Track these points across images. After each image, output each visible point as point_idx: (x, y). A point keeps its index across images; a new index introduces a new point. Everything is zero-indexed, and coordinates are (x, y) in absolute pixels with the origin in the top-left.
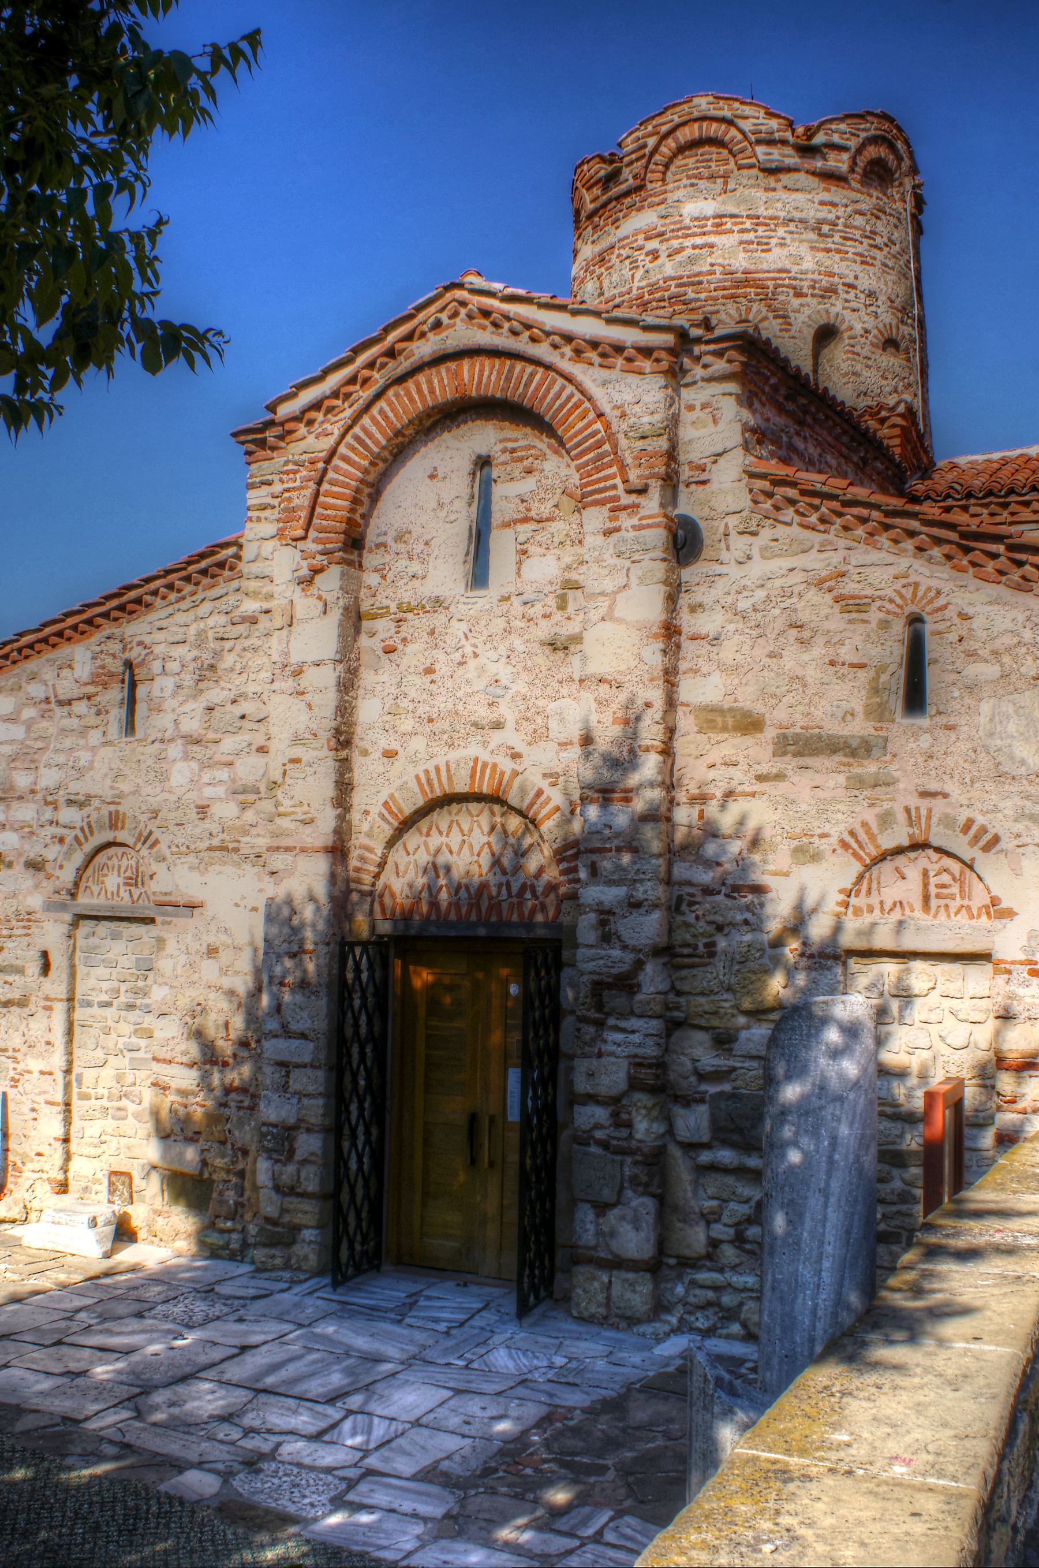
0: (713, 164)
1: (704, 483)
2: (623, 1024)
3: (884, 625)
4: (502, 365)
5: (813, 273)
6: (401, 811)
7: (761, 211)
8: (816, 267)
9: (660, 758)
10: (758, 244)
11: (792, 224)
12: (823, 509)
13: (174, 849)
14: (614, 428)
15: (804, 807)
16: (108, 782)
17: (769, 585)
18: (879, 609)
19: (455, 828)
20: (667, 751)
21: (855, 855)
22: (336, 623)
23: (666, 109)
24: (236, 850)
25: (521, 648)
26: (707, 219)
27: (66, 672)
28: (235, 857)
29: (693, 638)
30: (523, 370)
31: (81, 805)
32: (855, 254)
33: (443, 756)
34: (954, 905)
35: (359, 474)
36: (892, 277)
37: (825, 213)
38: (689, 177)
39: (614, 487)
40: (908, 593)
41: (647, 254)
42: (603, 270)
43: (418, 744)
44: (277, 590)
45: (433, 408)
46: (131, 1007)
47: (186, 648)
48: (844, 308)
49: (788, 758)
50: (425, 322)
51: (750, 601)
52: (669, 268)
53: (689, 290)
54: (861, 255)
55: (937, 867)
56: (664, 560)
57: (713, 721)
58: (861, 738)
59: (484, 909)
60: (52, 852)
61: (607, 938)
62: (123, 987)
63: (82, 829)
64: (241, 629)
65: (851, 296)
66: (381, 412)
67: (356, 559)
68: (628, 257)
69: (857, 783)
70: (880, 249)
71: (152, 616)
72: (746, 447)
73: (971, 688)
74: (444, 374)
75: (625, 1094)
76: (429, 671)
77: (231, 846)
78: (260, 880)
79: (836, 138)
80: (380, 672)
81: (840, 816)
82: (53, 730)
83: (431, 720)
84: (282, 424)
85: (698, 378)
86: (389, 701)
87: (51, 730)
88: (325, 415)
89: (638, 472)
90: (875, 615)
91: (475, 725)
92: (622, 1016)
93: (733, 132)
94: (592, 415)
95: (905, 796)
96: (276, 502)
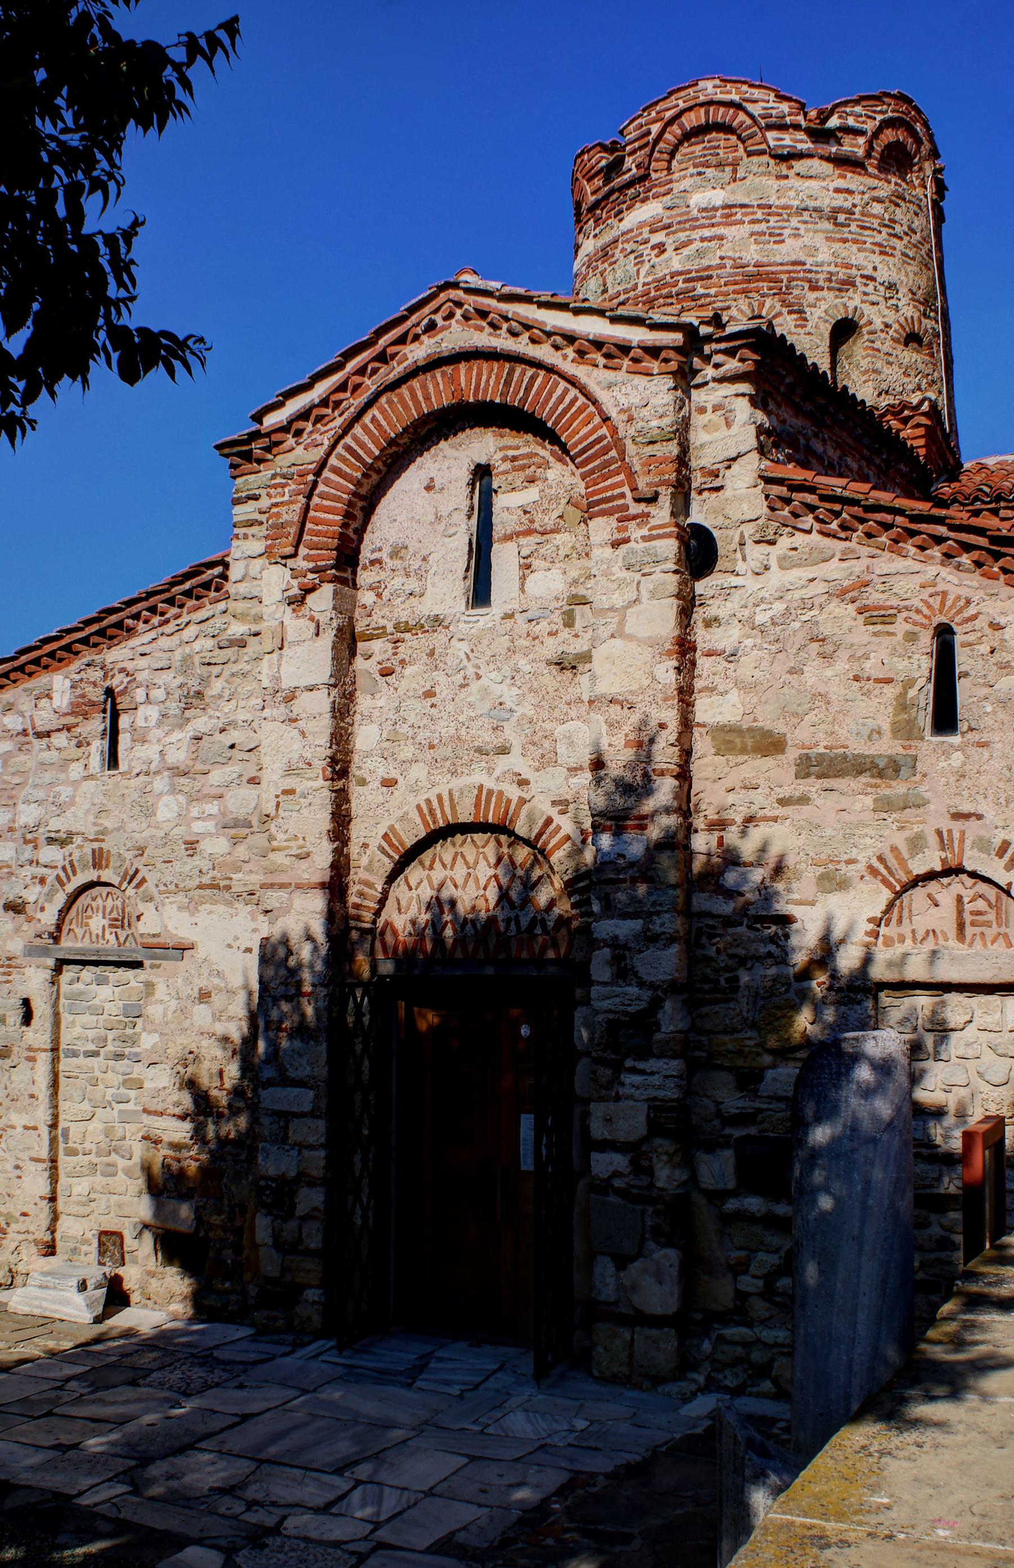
0: (721, 152)
1: (718, 489)
2: (641, 1065)
3: (911, 637)
5: (829, 265)
6: (402, 844)
8: (832, 259)
9: (676, 783)
10: (771, 235)
11: (805, 213)
12: (844, 515)
13: (162, 888)
14: (621, 434)
15: (829, 832)
16: (91, 818)
17: (788, 596)
18: (906, 620)
19: (459, 860)
20: (684, 775)
21: (885, 882)
22: (330, 645)
23: (671, 94)
24: (228, 888)
25: (527, 668)
26: (715, 209)
27: (44, 702)
28: (227, 896)
29: (709, 654)
30: (523, 373)
31: (63, 843)
33: (445, 784)
34: (990, 932)
35: (352, 487)
36: (913, 267)
37: (840, 201)
38: (695, 166)
39: (623, 496)
40: (936, 602)
41: (653, 248)
42: (606, 265)
43: (418, 772)
44: (266, 611)
45: (430, 414)
46: (119, 1056)
47: (171, 674)
48: (862, 302)
49: (812, 780)
50: (418, 324)
51: (770, 614)
52: (676, 263)
53: (698, 285)
54: (879, 245)
56: (676, 572)
57: (730, 742)
58: (889, 757)
59: (491, 947)
60: (30, 896)
61: (623, 973)
62: (111, 1035)
63: (64, 868)
64: (229, 652)
65: (870, 289)
66: (374, 419)
67: (350, 577)
68: (633, 252)
69: (885, 806)
70: (900, 238)
71: (134, 642)
72: (762, 450)
74: (439, 379)
75: (644, 1140)
77: (222, 883)
78: (254, 919)
79: (851, 122)
80: (377, 696)
81: (868, 840)
82: (31, 764)
83: (432, 747)
84: (268, 435)
85: (709, 378)
86: (388, 727)
87: (29, 764)
88: (314, 425)
89: (647, 479)
90: (901, 627)
91: (479, 750)
93: (742, 116)
94: (597, 420)
96: (263, 518)
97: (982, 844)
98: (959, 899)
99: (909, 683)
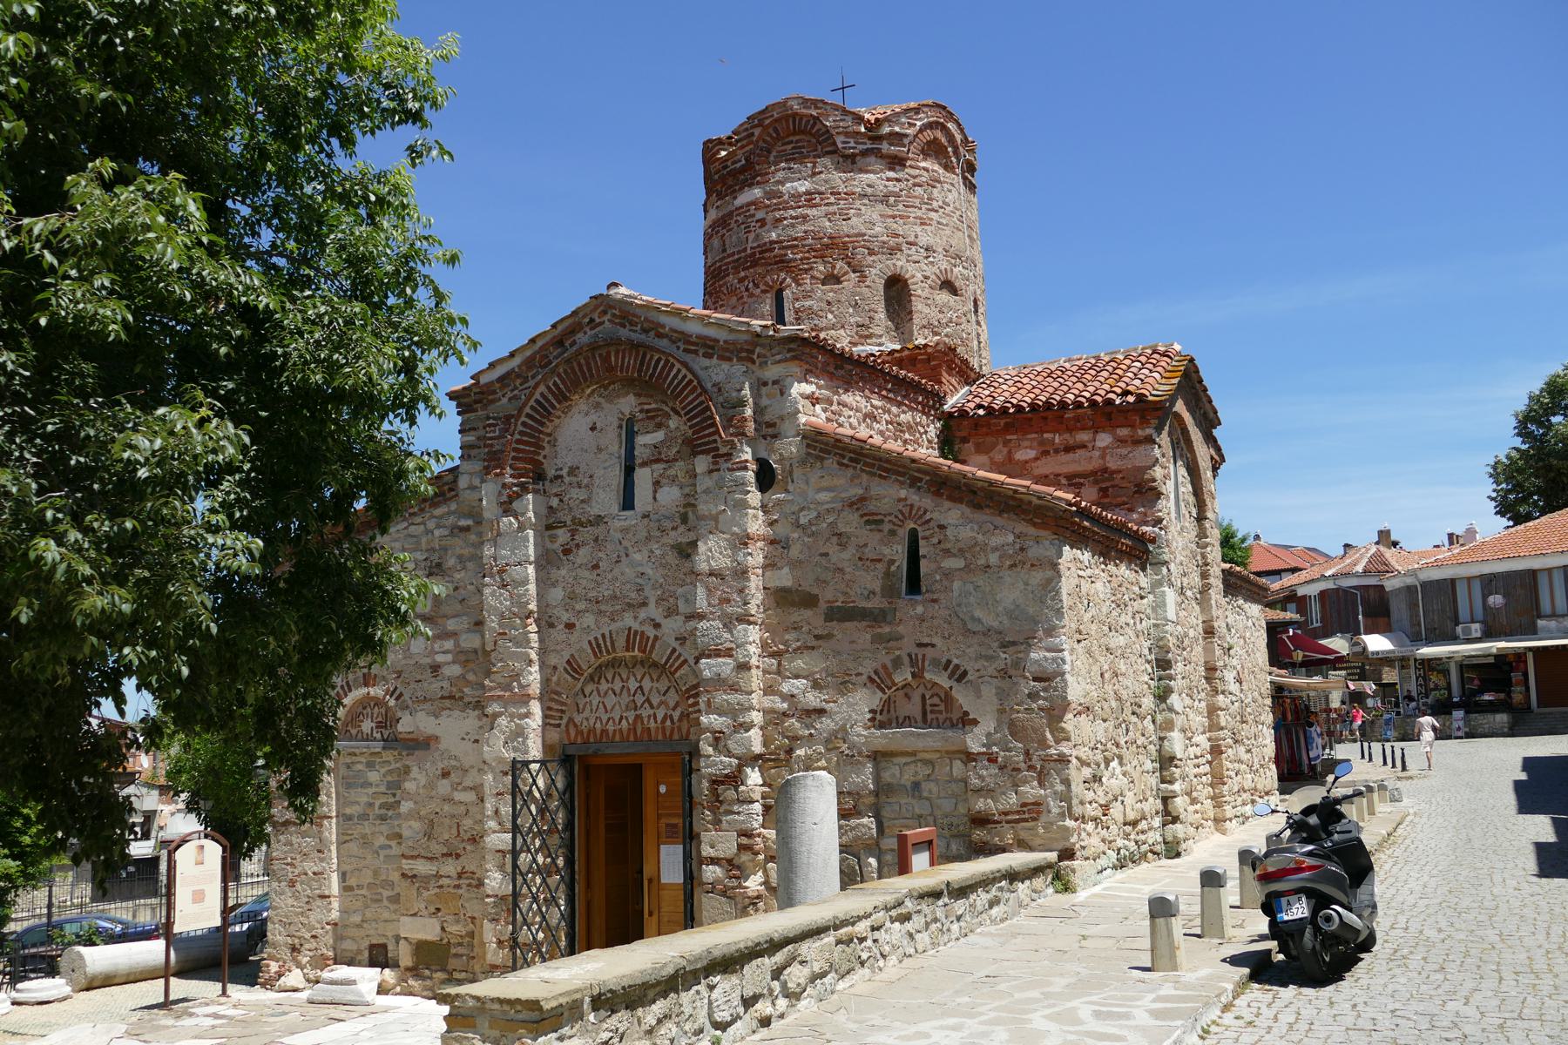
4: (637, 355)
19: (617, 677)
21: (879, 687)
24: (461, 698)
39: (715, 441)
40: (906, 511)
43: (589, 620)
55: (930, 693)
63: (342, 687)
66: (555, 384)
69: (878, 639)
70: (937, 211)
73: (948, 575)
76: (596, 567)
79: (897, 129)
83: (597, 602)
90: (886, 527)
91: (629, 605)
92: (732, 803)
95: (908, 646)
97: (935, 662)
98: (923, 697)
99: (892, 562)
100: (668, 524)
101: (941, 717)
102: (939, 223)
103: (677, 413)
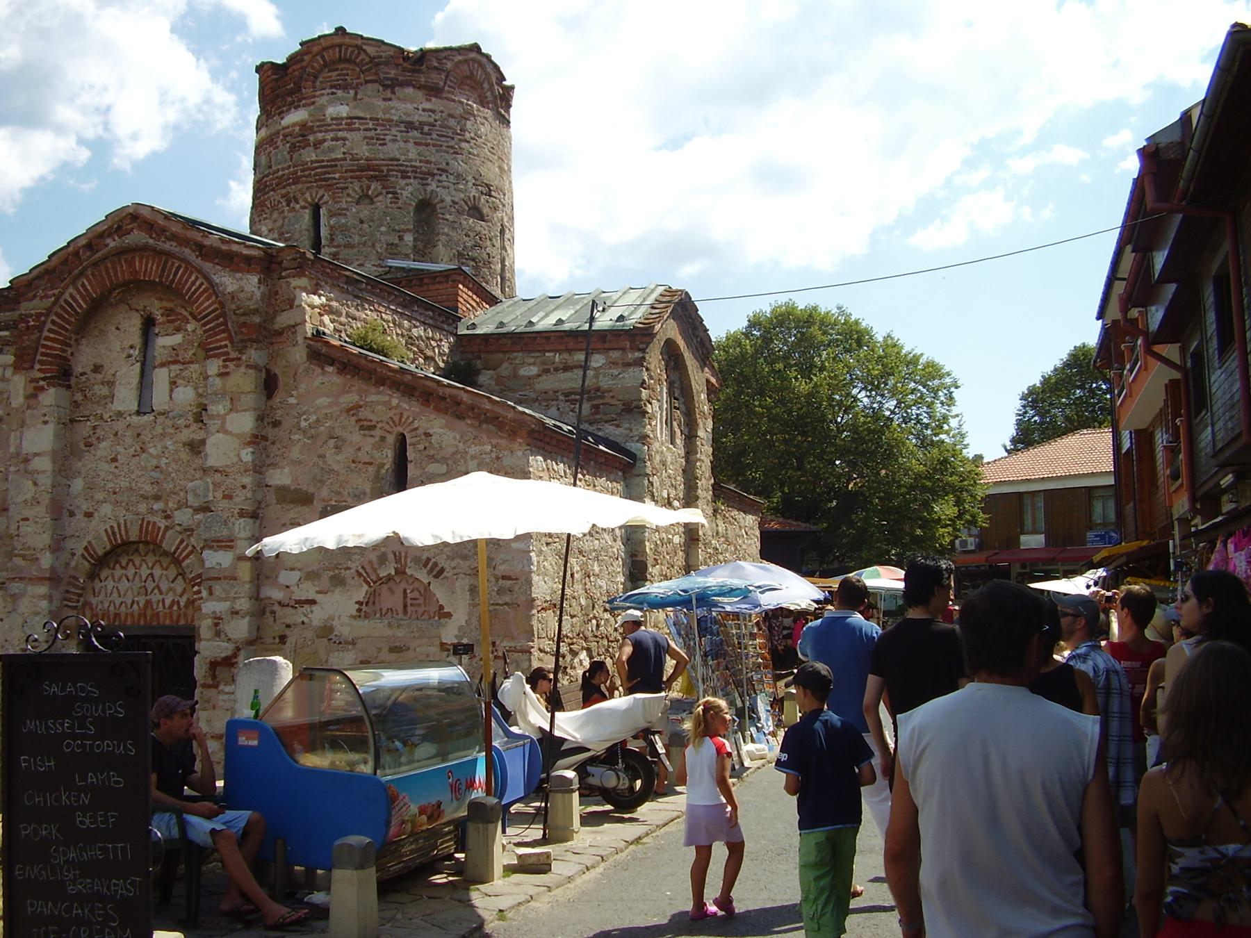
3: (383, 439)
4: (160, 261)
7: (380, 115)
10: (377, 139)
11: (402, 125)
19: (131, 564)
21: (365, 580)
26: (342, 119)
32: (447, 147)
34: (421, 610)
38: (331, 87)
39: (226, 346)
40: (396, 419)
42: (271, 149)
48: (437, 187)
54: (452, 147)
55: (411, 587)
61: (218, 634)
65: (444, 177)
66: (83, 285)
70: (469, 142)
76: (114, 460)
81: (356, 556)
83: (115, 493)
90: (378, 433)
91: (142, 496)
98: (405, 591)
99: (382, 465)
100: (181, 422)
101: (421, 610)
102: (470, 153)
103: (194, 317)
